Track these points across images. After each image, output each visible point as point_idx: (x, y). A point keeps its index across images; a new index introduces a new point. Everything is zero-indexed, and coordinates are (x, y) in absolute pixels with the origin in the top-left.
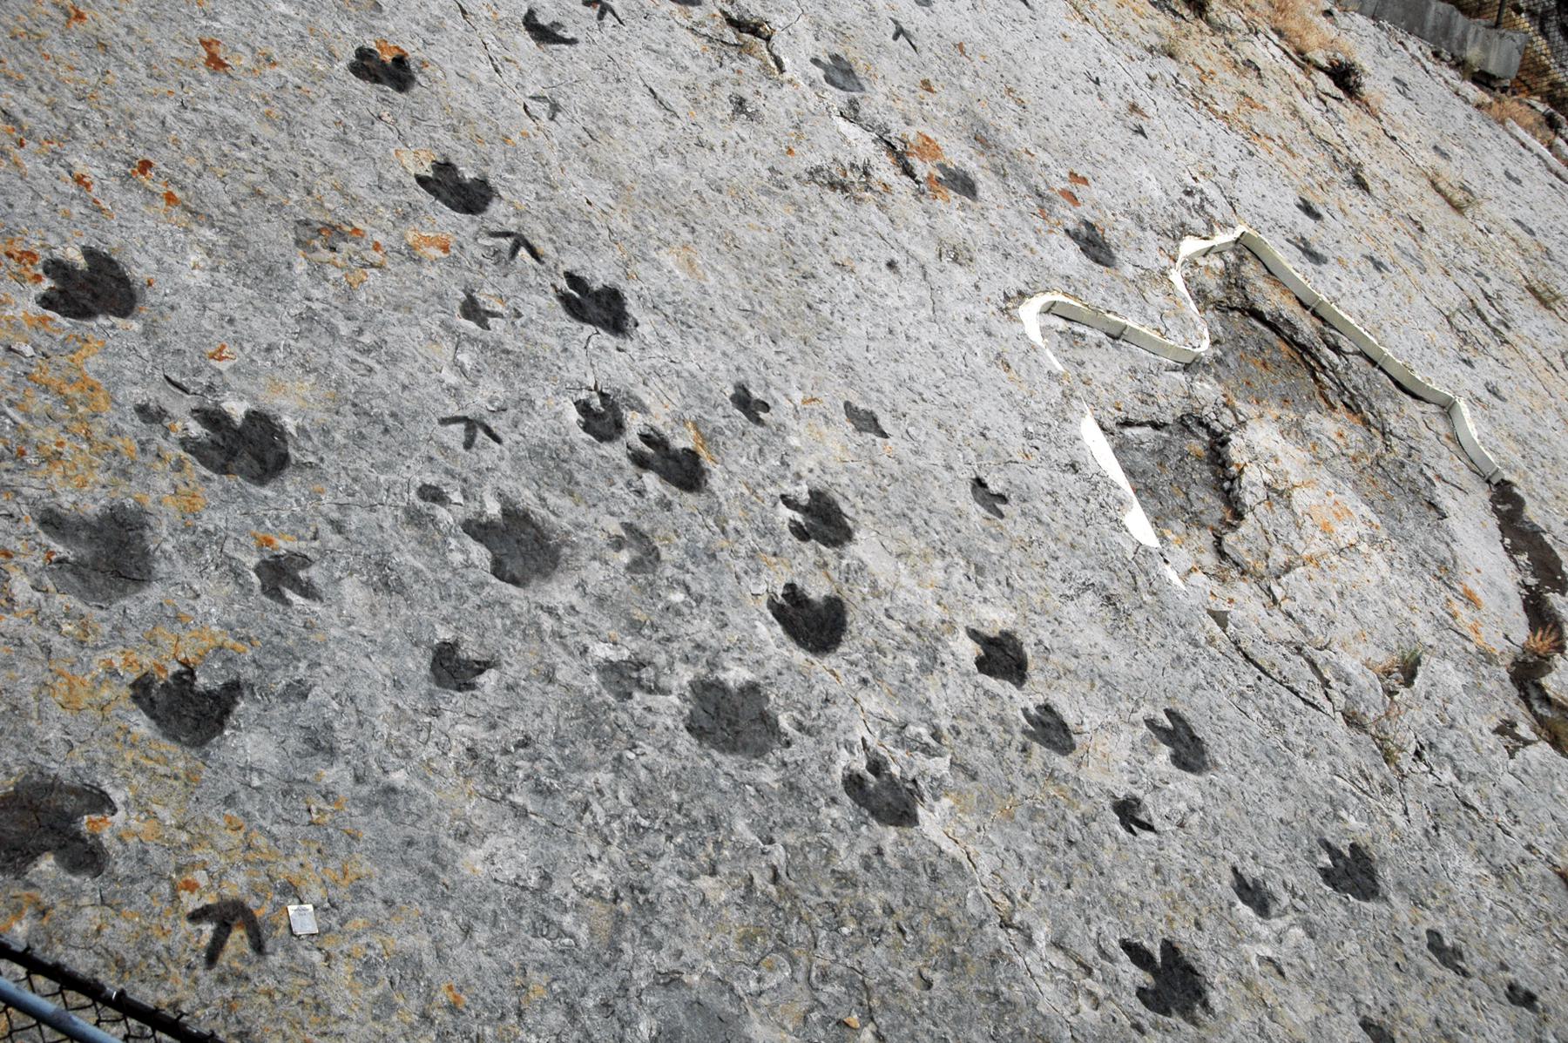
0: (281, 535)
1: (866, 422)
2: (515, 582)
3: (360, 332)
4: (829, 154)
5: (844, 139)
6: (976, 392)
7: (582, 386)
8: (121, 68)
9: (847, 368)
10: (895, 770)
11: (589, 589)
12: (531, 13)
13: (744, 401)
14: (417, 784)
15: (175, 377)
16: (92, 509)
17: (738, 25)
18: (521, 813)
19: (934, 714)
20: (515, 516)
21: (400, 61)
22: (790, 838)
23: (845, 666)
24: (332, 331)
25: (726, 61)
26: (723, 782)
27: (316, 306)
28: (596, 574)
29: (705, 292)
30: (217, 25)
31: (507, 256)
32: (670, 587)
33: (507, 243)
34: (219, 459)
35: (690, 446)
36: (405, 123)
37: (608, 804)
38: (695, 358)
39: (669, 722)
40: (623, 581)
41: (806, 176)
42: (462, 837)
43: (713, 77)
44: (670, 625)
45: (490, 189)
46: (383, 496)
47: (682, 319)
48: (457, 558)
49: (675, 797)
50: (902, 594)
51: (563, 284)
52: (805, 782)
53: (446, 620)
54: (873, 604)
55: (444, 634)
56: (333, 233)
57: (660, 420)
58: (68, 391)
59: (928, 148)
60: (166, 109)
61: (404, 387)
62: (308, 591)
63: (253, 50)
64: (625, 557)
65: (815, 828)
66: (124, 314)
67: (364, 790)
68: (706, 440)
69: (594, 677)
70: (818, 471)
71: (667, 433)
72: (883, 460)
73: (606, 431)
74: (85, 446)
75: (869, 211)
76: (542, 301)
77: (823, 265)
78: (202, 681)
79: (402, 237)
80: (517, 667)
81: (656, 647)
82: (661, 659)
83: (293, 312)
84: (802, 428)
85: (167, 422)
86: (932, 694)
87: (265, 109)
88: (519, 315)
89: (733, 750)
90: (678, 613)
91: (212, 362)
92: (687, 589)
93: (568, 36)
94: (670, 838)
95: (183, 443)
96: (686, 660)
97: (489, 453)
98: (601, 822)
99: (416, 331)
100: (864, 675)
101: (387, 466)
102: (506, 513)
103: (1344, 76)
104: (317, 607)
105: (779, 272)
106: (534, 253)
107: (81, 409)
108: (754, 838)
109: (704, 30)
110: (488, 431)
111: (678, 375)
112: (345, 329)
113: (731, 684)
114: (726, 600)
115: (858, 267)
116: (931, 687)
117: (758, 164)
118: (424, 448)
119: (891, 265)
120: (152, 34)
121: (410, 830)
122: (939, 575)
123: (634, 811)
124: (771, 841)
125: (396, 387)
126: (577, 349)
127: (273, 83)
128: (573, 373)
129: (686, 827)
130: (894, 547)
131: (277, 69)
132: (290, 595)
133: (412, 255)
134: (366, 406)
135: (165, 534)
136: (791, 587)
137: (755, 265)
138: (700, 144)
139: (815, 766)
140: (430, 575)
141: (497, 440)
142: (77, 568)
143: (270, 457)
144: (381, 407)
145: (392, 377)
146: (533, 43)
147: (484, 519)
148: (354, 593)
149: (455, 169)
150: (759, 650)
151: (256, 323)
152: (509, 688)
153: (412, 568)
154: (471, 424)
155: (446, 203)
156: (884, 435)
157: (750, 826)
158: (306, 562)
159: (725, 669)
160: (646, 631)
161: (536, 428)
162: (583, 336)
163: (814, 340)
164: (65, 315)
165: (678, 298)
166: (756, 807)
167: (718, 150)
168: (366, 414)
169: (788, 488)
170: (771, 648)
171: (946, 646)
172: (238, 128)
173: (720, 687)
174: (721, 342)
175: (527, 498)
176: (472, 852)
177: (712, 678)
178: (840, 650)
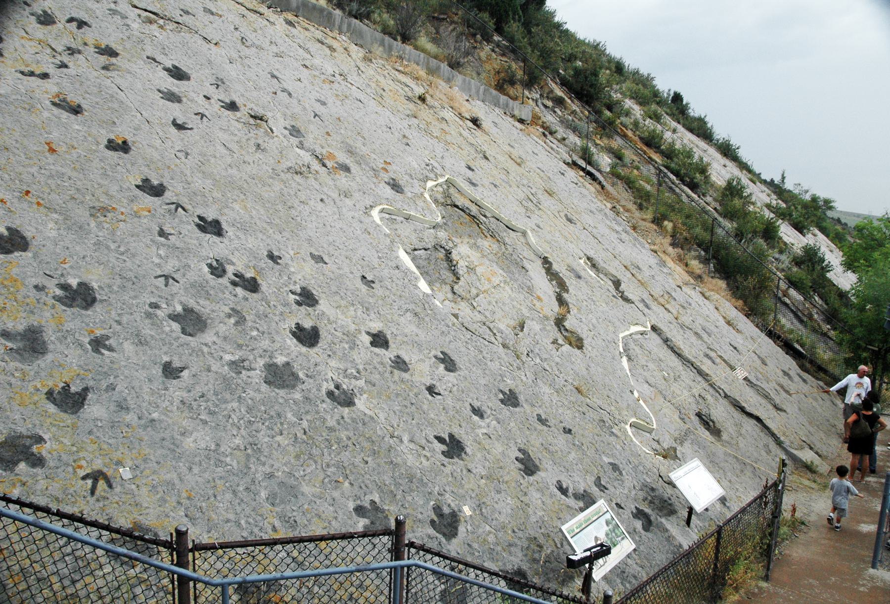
0: (97, 329)
1: (319, 259)
2: (190, 335)
3: (119, 247)
4: (294, 162)
5: (299, 155)
6: (358, 244)
7: (208, 258)
8: (14, 156)
9: (309, 240)
10: (345, 387)
11: (220, 334)
12: (174, 120)
13: (271, 257)
14: (163, 417)
15: (48, 272)
16: (21, 328)
17: (254, 117)
18: (205, 422)
19: (357, 364)
20: (188, 311)
21: (125, 142)
22: (309, 417)
23: (321, 351)
24: (108, 248)
25: (251, 131)
26: (281, 401)
27: (101, 239)
28: (222, 328)
29: (252, 217)
30: (52, 136)
31: (174, 211)
32: (251, 330)
33: (173, 206)
34: (69, 303)
35: (253, 276)
36: (129, 166)
37: (238, 414)
38: (251, 242)
39: (257, 381)
40: (233, 330)
41: (286, 170)
42: (183, 434)
43: (246, 137)
44: (254, 344)
45: (164, 187)
46: (135, 309)
47: (244, 228)
48: (167, 329)
49: (263, 408)
50: (340, 322)
51: (197, 220)
52: (311, 396)
53: (166, 353)
54: (329, 326)
55: (166, 359)
56: (104, 210)
57: (240, 268)
58: (6, 283)
59: (331, 156)
60: (34, 170)
61: (139, 266)
62: (111, 349)
63: (66, 144)
64: (232, 320)
65: (317, 412)
66: (25, 250)
67: (143, 422)
68: (258, 273)
69: (226, 368)
70: (302, 279)
71: (243, 272)
72: (327, 273)
73: (220, 273)
74: (15, 303)
75: (311, 181)
76: (189, 227)
77: (296, 203)
78: (73, 389)
79: (132, 209)
81: (249, 353)
82: (251, 357)
83: (92, 242)
84: (295, 264)
85: (47, 290)
86: (355, 357)
87: (73, 166)
88: (181, 234)
89: (283, 387)
90: (256, 339)
91: (62, 265)
92: (258, 330)
93: (189, 127)
94: (263, 424)
95: (54, 297)
96: (261, 356)
97: (174, 287)
98: (236, 421)
99: (141, 244)
100: (329, 353)
101: (136, 297)
102: (184, 310)
103: (475, 121)
104: (114, 354)
105: (280, 207)
107: (12, 289)
108: (295, 419)
109: (242, 120)
110: (173, 279)
111: (245, 249)
112: (113, 246)
113: (279, 363)
114: (273, 332)
115: (309, 202)
116: (355, 355)
117: (267, 168)
118: (149, 288)
119: (322, 200)
120: (26, 142)
121: (162, 435)
122: (353, 313)
123: (248, 416)
124: (302, 420)
125: (136, 266)
126: (205, 244)
127: (75, 155)
128: (204, 253)
129: (269, 419)
130: (334, 305)
131: (77, 150)
132: (103, 351)
133: (137, 215)
134: (125, 275)
135: (51, 334)
136: (297, 324)
137: (270, 205)
138: (244, 162)
139: (315, 390)
140: (157, 337)
141: (177, 282)
142: (17, 351)
143: (89, 299)
144: (130, 274)
145: (133, 263)
146: (176, 131)
147: (176, 313)
148: (128, 347)
149: (150, 181)
150: (288, 349)
151: (78, 248)
152: (194, 376)
153: (150, 335)
154: (166, 277)
155: (148, 194)
156: (326, 263)
157: (293, 415)
158: (108, 338)
159: (276, 358)
160: (244, 348)
161: (192, 276)
162: (207, 238)
163: (296, 231)
165: (242, 221)
166: (295, 408)
167: (252, 164)
168: (125, 278)
169: (292, 287)
170: (293, 348)
171: (358, 339)
172: (63, 174)
173: (275, 365)
174: (260, 235)
175: (192, 303)
176: (188, 440)
177: (271, 362)
178: (319, 345)
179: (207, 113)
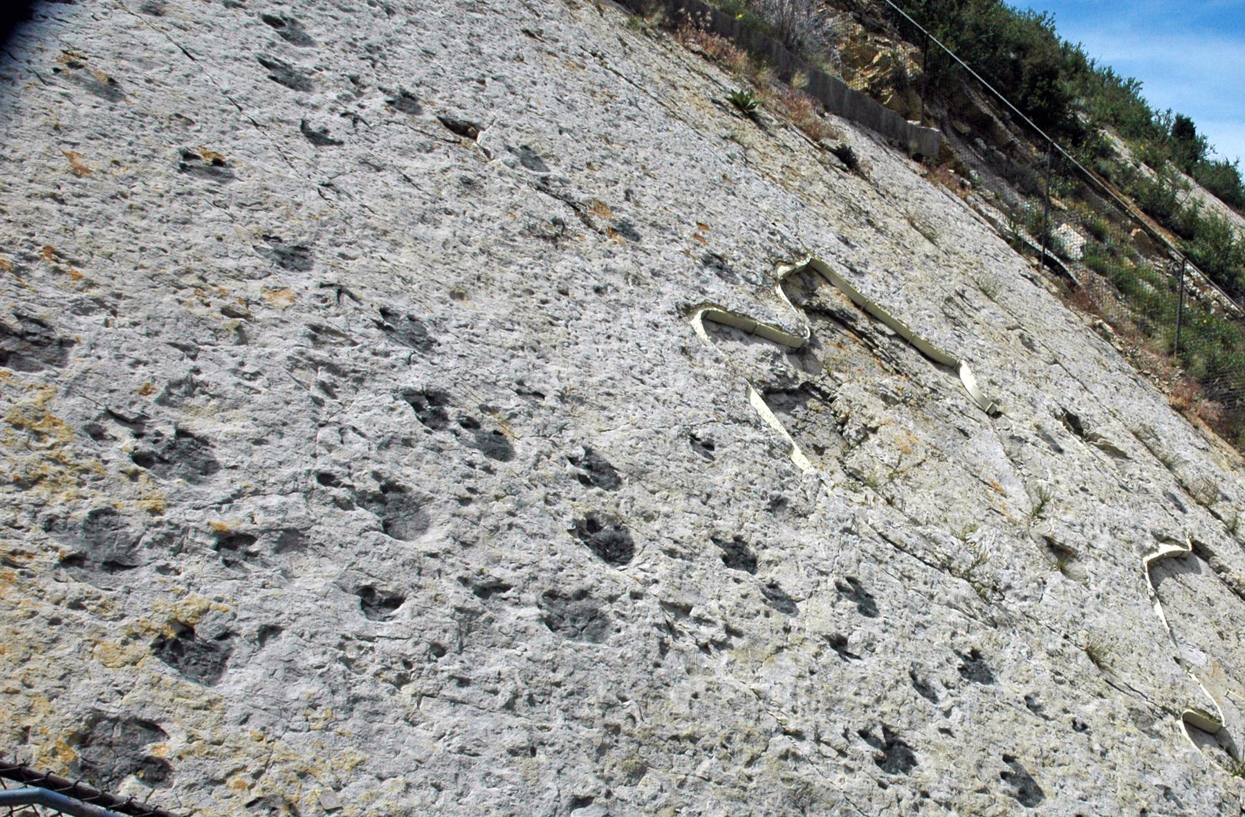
33: (332, 293)
80: (423, 599)
91: (143, 397)
106: (352, 296)
110: (354, 429)
141: (363, 435)
164: (19, 368)
169: (567, 450)
179: (362, 115)
